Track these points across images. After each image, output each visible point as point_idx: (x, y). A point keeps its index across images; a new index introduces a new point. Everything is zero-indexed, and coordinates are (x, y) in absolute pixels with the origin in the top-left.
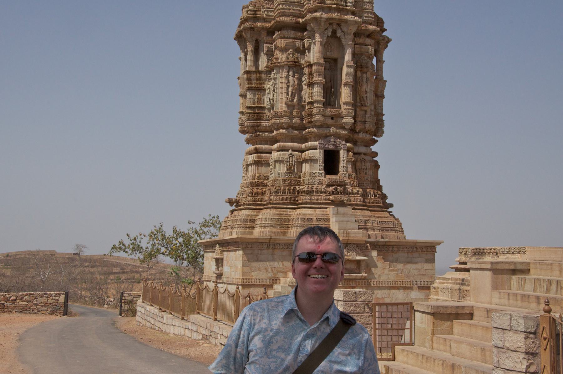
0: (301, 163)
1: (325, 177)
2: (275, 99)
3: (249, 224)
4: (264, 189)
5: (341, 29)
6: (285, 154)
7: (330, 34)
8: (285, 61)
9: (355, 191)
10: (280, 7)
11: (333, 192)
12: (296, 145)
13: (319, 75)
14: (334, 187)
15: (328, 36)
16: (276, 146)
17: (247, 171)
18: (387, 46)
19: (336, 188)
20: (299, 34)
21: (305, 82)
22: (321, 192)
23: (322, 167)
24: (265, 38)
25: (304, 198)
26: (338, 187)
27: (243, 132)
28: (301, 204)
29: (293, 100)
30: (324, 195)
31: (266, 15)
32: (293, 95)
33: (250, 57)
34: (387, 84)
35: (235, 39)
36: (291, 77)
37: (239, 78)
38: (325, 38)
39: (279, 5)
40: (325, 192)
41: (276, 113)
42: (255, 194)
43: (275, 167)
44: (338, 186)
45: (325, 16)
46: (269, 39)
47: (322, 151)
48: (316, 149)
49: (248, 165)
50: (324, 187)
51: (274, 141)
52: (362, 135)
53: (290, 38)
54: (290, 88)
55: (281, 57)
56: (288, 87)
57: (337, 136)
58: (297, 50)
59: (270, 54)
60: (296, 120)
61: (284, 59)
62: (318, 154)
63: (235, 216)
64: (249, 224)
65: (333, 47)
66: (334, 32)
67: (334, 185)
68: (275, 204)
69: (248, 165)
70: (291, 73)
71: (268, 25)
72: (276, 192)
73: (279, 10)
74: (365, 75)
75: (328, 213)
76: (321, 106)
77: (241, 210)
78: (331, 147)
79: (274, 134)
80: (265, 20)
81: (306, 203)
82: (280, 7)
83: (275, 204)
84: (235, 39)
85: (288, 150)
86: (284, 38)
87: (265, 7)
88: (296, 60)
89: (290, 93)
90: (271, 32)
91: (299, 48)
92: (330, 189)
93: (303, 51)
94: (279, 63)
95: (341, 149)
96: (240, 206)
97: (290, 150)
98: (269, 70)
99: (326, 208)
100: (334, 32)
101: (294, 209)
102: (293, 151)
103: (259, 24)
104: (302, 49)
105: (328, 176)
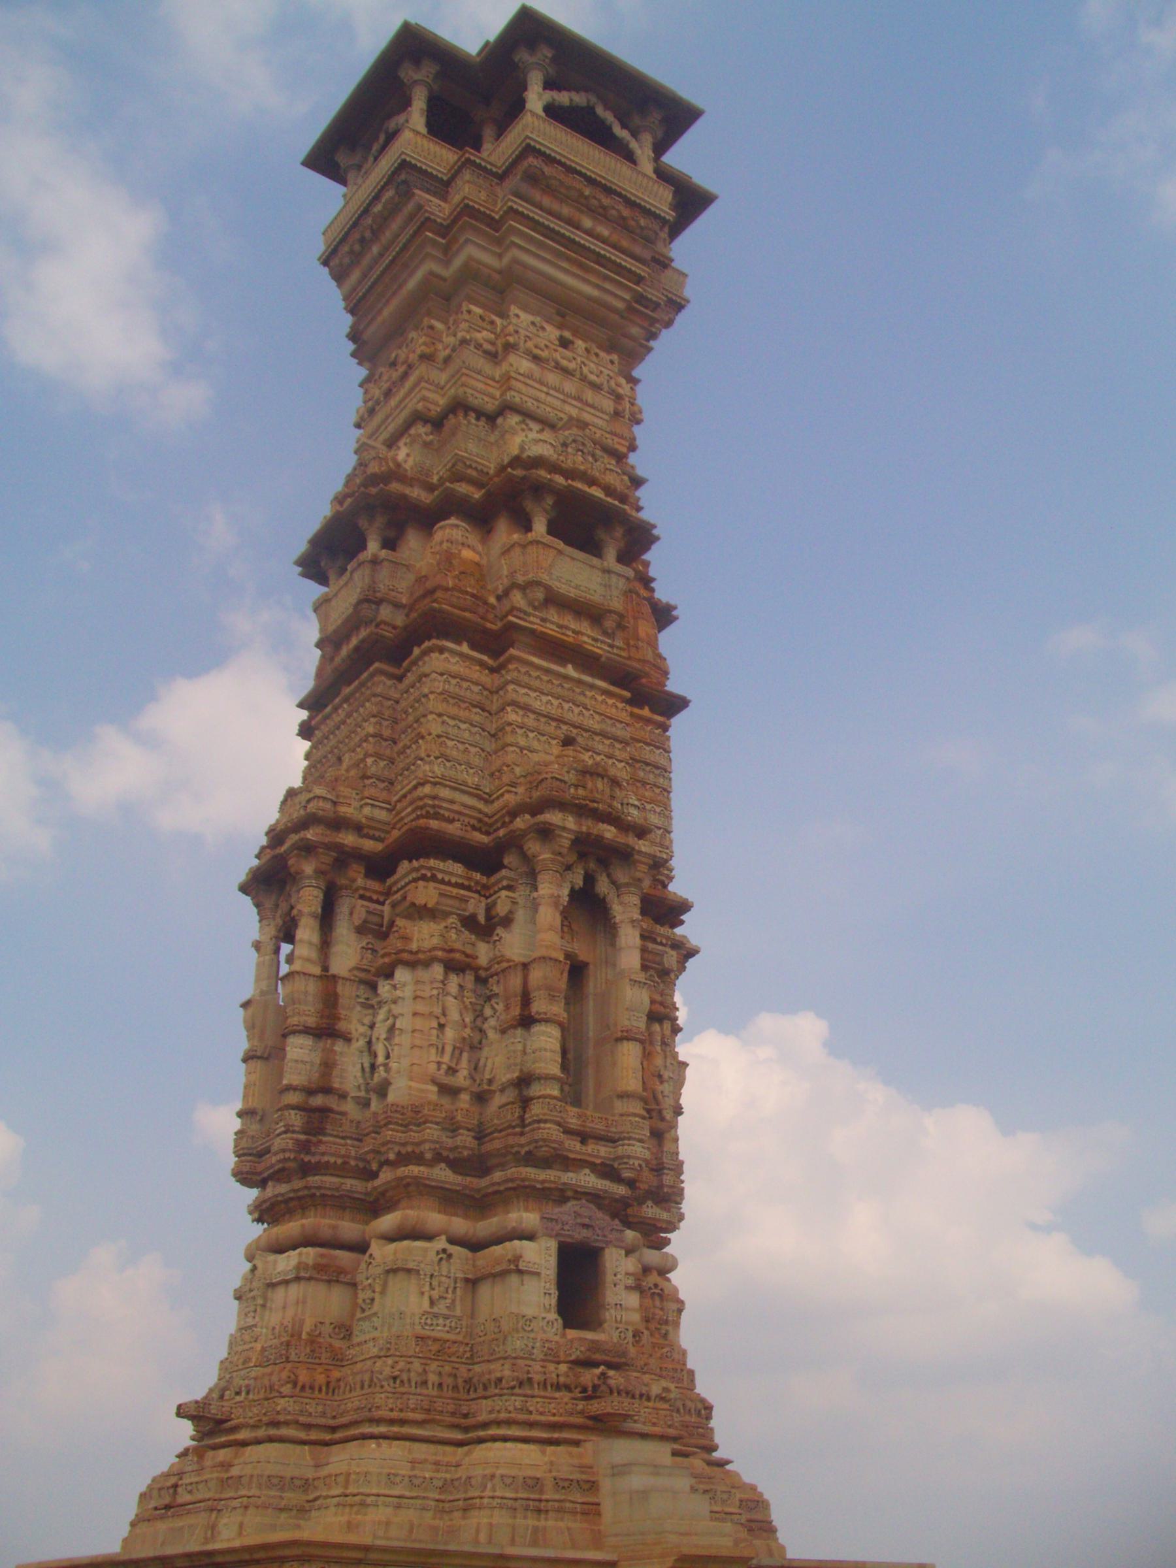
0: (473, 1283)
1: (564, 1335)
2: (394, 1065)
3: (293, 1497)
4: (336, 1374)
5: (609, 876)
6: (426, 1250)
7: (579, 882)
8: (434, 949)
9: (655, 1390)
10: (427, 789)
11: (595, 1387)
12: (460, 1225)
13: (552, 998)
14: (598, 1371)
15: (572, 890)
16: (388, 1221)
17: (264, 1306)
18: (684, 968)
19: (603, 1374)
20: (477, 876)
21: (492, 1022)
22: (558, 1387)
23: (554, 1300)
24: (360, 882)
25: (499, 1403)
26: (611, 1373)
27: (244, 1177)
28: (485, 1425)
29: (452, 1071)
30: (564, 1396)
31: (367, 818)
32: (458, 1051)
33: (307, 932)
34: (689, 1072)
35: (244, 889)
36: (451, 1002)
37: (246, 1005)
38: (566, 892)
39: (423, 784)
40: (568, 1388)
41: (396, 1108)
42: (303, 1388)
43: (383, 1292)
44: (610, 1366)
45: (570, 822)
46: (374, 885)
47: (553, 1245)
48: (531, 1237)
49: (272, 1285)
50: (563, 1368)
51: (374, 1207)
52: (650, 1211)
53: (449, 884)
54: (450, 1034)
55: (425, 935)
56: (441, 1026)
57: (595, 1198)
58: (469, 922)
59: (376, 931)
60: (465, 1139)
61: (436, 941)
62: (541, 1255)
63: (226, 1466)
64: (293, 1497)
65: (574, 927)
66: (589, 879)
67: (596, 1364)
68: (392, 1422)
69: (272, 1285)
70: (453, 988)
71: (369, 845)
72: (395, 1378)
73: (421, 799)
74: (656, 1027)
75: (587, 1461)
76: (556, 1093)
77: (244, 1444)
78: (581, 1234)
79: (377, 1182)
80: (358, 828)
81: (509, 1423)
82: (427, 789)
83: (392, 1422)
84: (244, 889)
85: (429, 1237)
86: (434, 878)
87: (366, 794)
88: (469, 950)
89: (449, 1049)
90: (380, 867)
91: (473, 917)
92: (589, 1376)
93: (486, 927)
94: (411, 952)
95: (608, 1243)
96: (235, 1429)
97: (444, 1237)
98: (372, 978)
99: (577, 1443)
100: (589, 879)
101: (460, 1444)
102: (452, 1241)
103: (349, 839)
104: (482, 919)
105: (572, 1333)
